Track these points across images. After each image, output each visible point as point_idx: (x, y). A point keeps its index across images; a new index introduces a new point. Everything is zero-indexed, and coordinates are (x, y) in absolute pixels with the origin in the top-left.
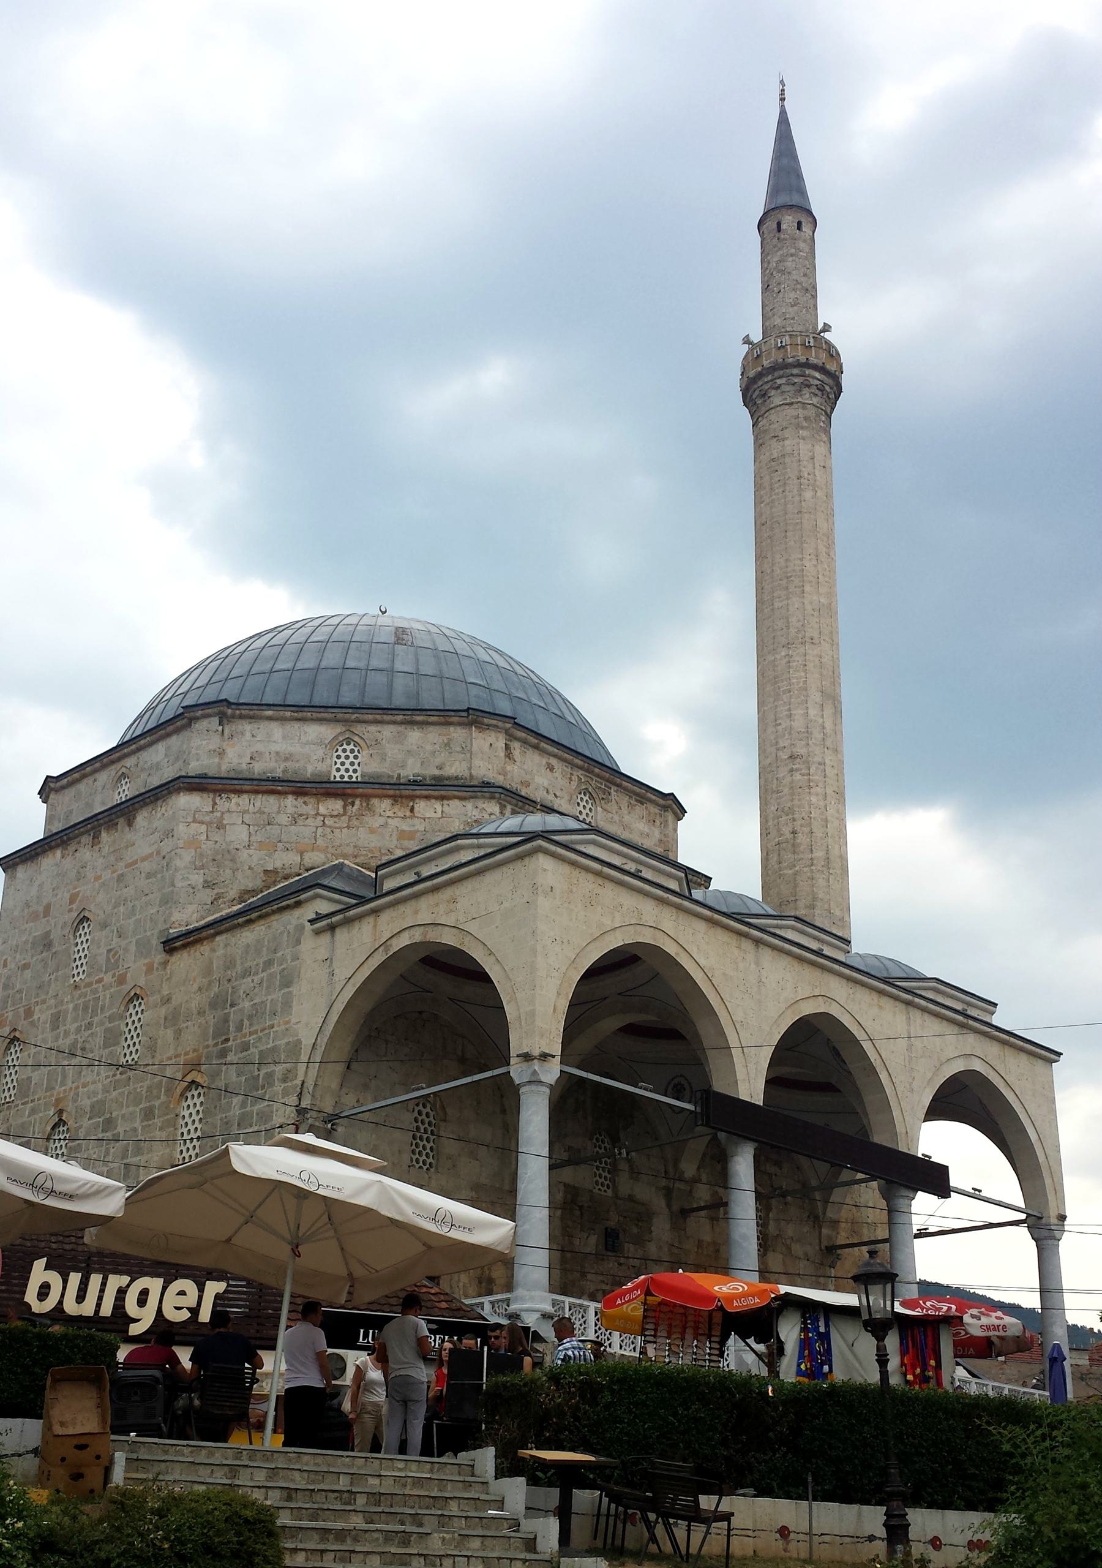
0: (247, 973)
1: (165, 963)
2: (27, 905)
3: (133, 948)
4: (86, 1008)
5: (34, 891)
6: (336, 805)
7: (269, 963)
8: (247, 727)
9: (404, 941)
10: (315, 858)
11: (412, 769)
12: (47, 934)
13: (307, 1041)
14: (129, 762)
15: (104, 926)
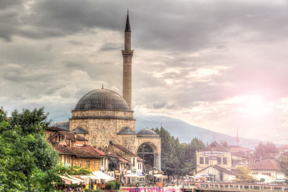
0: (128, 139)
1: (117, 136)
2: (93, 124)
3: (112, 132)
4: (105, 137)
5: (94, 123)
6: (126, 121)
7: (131, 139)
8: (118, 112)
9: (147, 141)
10: (125, 126)
11: (128, 116)
12: (98, 128)
13: (136, 147)
14: (104, 111)
15: (107, 129)
